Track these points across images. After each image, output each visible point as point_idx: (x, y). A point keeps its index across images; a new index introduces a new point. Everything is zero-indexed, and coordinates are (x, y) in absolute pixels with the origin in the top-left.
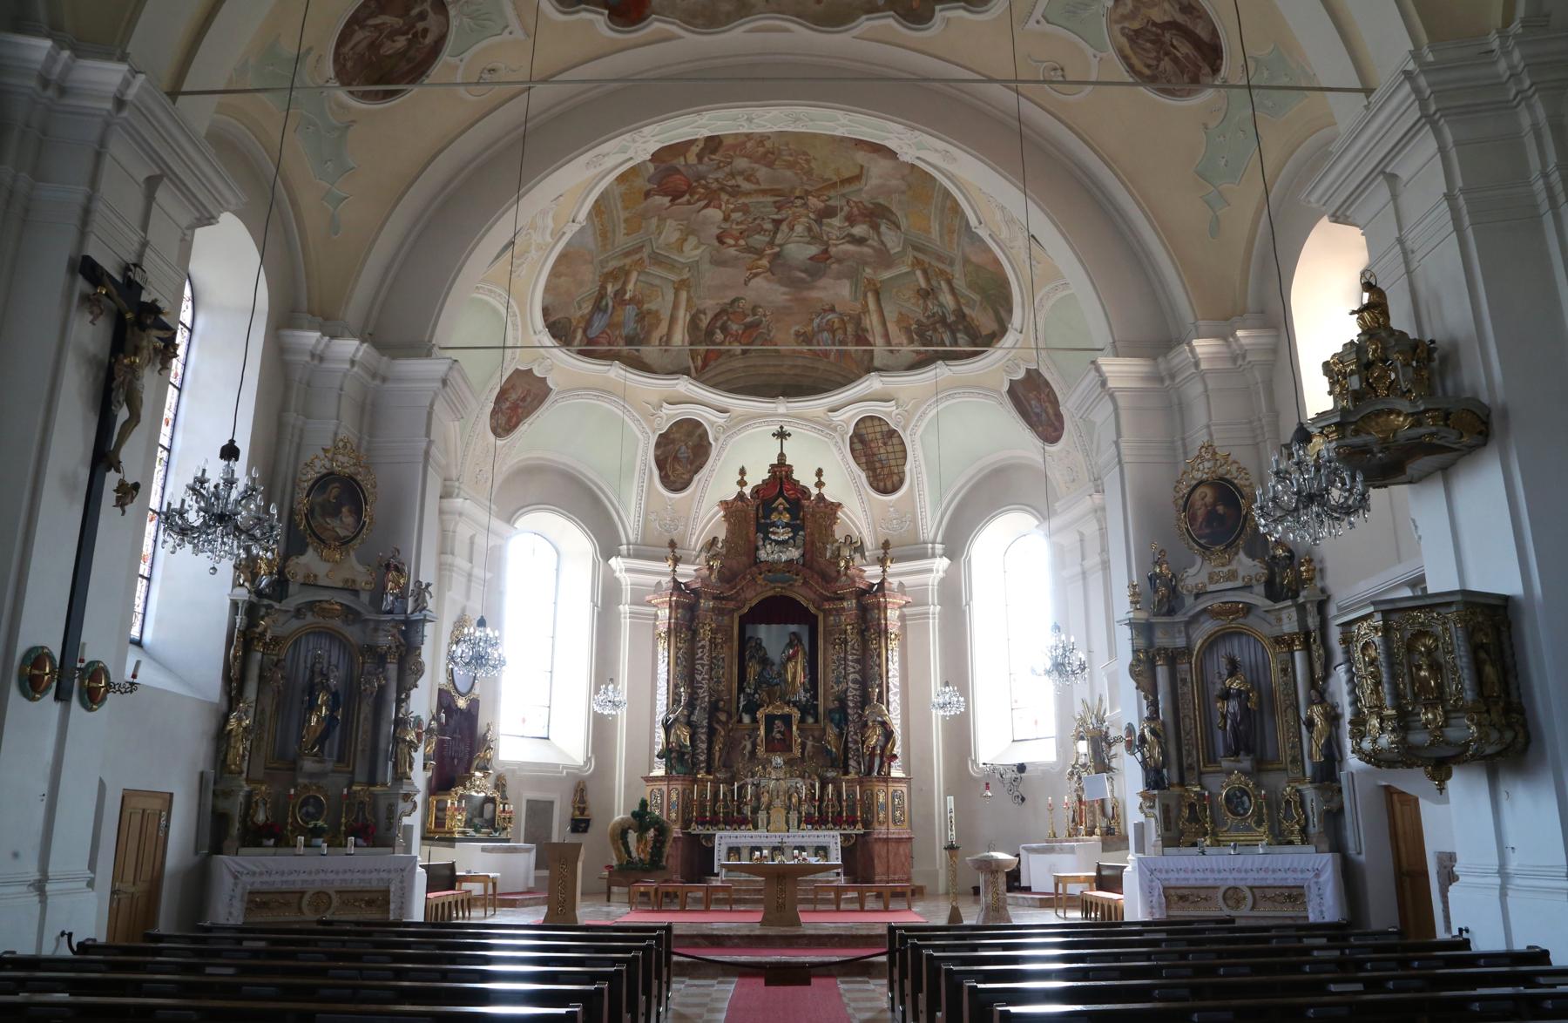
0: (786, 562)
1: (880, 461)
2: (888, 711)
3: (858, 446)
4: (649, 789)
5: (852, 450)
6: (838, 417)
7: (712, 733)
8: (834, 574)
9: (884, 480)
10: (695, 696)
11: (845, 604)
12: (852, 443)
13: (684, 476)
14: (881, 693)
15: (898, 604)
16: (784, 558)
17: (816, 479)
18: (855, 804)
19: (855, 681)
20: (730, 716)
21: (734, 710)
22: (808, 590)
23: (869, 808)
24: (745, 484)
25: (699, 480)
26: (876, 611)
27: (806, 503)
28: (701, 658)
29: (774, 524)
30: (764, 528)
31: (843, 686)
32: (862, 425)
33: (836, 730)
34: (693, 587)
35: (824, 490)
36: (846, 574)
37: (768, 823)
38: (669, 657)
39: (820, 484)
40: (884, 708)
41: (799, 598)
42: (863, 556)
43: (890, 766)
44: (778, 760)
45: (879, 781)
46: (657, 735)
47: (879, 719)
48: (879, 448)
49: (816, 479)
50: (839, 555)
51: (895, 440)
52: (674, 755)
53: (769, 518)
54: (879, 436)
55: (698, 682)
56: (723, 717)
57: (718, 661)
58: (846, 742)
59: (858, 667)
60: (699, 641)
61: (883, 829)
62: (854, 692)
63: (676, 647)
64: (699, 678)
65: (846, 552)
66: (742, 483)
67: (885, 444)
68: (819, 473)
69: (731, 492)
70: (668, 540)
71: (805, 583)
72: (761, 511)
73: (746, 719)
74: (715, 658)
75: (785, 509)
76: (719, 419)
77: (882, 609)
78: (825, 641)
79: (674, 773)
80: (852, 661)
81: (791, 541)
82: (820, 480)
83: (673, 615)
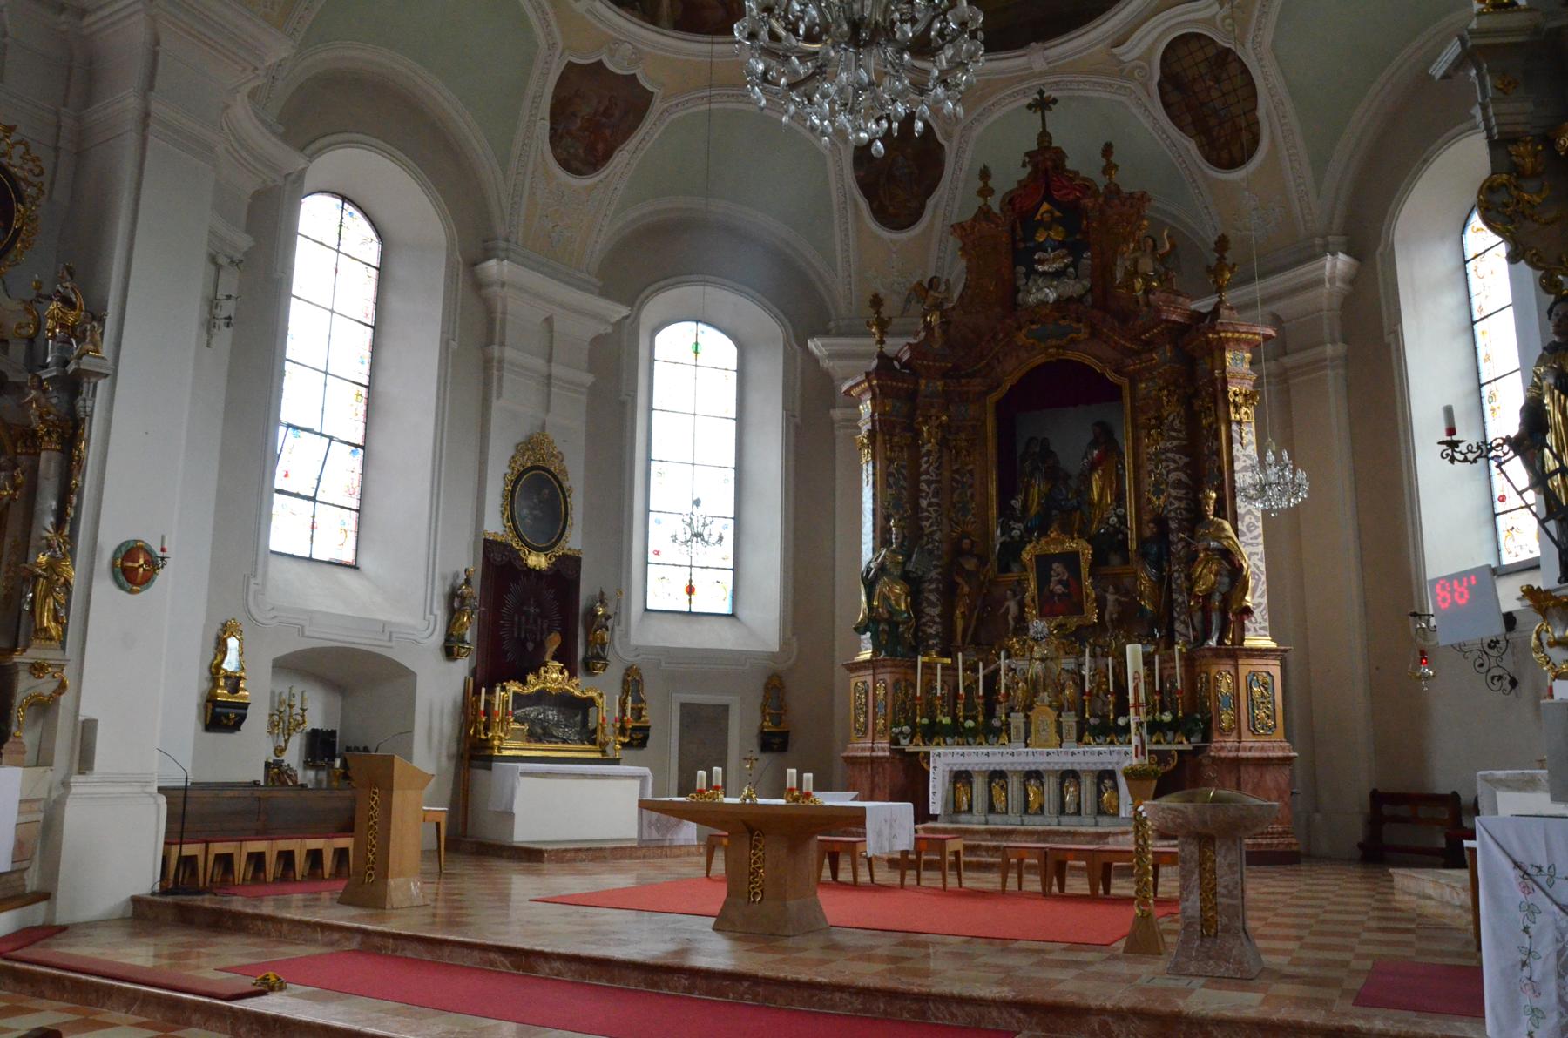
2: (1236, 530)
5: (1167, 106)
6: (1131, 52)
7: (949, 593)
14: (1220, 502)
15: (1248, 342)
17: (1103, 162)
24: (991, 192)
25: (936, 206)
26: (1208, 359)
27: (1088, 202)
28: (927, 472)
29: (1041, 247)
30: (1023, 256)
35: (1117, 177)
36: (1148, 304)
39: (1109, 168)
40: (1227, 525)
41: (1090, 361)
47: (1213, 544)
49: (1103, 162)
52: (882, 626)
54: (1203, 70)
55: (923, 510)
56: (970, 564)
58: (1170, 591)
60: (923, 445)
61: (1230, 742)
63: (887, 459)
64: (924, 503)
66: (986, 192)
67: (1217, 80)
68: (1107, 150)
71: (1094, 334)
74: (957, 471)
81: (1071, 270)
83: (878, 409)
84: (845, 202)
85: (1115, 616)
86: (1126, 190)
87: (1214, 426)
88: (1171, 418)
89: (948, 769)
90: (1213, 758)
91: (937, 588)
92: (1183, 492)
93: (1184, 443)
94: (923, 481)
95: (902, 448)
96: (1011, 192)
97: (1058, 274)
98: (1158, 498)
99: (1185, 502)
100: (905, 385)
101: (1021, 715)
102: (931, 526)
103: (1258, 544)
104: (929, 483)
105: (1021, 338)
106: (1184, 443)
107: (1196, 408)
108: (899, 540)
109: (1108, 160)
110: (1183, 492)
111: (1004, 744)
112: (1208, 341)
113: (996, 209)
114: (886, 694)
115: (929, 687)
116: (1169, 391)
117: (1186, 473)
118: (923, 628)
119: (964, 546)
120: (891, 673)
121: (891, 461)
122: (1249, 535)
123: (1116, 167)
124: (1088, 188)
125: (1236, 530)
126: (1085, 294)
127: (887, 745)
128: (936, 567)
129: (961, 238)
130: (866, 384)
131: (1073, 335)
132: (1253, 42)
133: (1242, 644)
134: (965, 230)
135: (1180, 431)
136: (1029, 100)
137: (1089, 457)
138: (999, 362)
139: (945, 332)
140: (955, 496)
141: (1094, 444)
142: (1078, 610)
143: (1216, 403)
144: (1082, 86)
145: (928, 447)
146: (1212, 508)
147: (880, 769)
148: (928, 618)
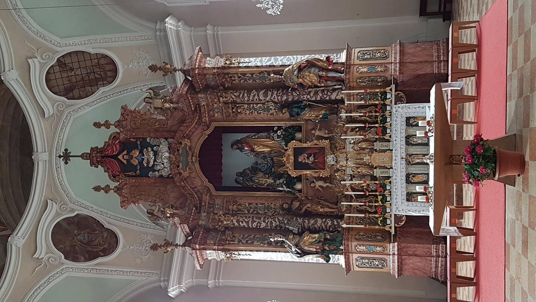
0: (170, 153)
2: (289, 65)
3: (76, 92)
5: (80, 98)
6: (49, 110)
7: (309, 214)
8: (181, 114)
14: (275, 73)
15: (201, 58)
16: (167, 155)
17: (103, 127)
19: (266, 95)
24: (108, 186)
26: (207, 76)
27: (122, 136)
28: (247, 223)
29: (141, 163)
31: (272, 106)
34: (188, 230)
37: (387, 168)
38: (246, 251)
39: (107, 125)
44: (330, 159)
46: (310, 261)
48: (76, 75)
50: (161, 108)
51: (68, 60)
53: (137, 166)
54: (65, 75)
56: (296, 204)
60: (234, 224)
64: (263, 225)
65: (158, 103)
66: (107, 189)
67: (72, 70)
68: (97, 125)
69: (115, 198)
70: (152, 251)
72: (130, 173)
74: (249, 211)
75: (128, 154)
76: (53, 209)
77: (205, 72)
78: (236, 121)
79: (342, 248)
81: (155, 148)
82: (104, 125)
84: (96, 269)
85: (326, 132)
86: (118, 117)
87: (240, 75)
88: (233, 97)
89: (406, 203)
90: (400, 73)
91: (307, 219)
92: (269, 92)
93: (246, 91)
94: (252, 226)
95: (233, 236)
96: (109, 176)
97: (156, 154)
98: (271, 109)
99: (274, 91)
100: (201, 232)
101: (375, 170)
103: (297, 57)
105: (186, 174)
106: (246, 91)
107: (230, 85)
108: (282, 236)
109: (102, 125)
110: (269, 92)
111: (390, 182)
112: (199, 74)
113: (117, 184)
114: (363, 245)
115: (361, 221)
118: (328, 227)
119: (287, 207)
121: (240, 241)
125: (289, 65)
126: (168, 142)
128: (296, 219)
129: (129, 203)
130: (198, 251)
131: (187, 148)
133: (344, 62)
134: (126, 201)
135: (240, 93)
136: (63, 163)
139: (176, 209)
140: (261, 212)
141: (241, 149)
142: (323, 148)
143: (228, 74)
144: (61, 137)
146: (278, 76)
148: (323, 224)
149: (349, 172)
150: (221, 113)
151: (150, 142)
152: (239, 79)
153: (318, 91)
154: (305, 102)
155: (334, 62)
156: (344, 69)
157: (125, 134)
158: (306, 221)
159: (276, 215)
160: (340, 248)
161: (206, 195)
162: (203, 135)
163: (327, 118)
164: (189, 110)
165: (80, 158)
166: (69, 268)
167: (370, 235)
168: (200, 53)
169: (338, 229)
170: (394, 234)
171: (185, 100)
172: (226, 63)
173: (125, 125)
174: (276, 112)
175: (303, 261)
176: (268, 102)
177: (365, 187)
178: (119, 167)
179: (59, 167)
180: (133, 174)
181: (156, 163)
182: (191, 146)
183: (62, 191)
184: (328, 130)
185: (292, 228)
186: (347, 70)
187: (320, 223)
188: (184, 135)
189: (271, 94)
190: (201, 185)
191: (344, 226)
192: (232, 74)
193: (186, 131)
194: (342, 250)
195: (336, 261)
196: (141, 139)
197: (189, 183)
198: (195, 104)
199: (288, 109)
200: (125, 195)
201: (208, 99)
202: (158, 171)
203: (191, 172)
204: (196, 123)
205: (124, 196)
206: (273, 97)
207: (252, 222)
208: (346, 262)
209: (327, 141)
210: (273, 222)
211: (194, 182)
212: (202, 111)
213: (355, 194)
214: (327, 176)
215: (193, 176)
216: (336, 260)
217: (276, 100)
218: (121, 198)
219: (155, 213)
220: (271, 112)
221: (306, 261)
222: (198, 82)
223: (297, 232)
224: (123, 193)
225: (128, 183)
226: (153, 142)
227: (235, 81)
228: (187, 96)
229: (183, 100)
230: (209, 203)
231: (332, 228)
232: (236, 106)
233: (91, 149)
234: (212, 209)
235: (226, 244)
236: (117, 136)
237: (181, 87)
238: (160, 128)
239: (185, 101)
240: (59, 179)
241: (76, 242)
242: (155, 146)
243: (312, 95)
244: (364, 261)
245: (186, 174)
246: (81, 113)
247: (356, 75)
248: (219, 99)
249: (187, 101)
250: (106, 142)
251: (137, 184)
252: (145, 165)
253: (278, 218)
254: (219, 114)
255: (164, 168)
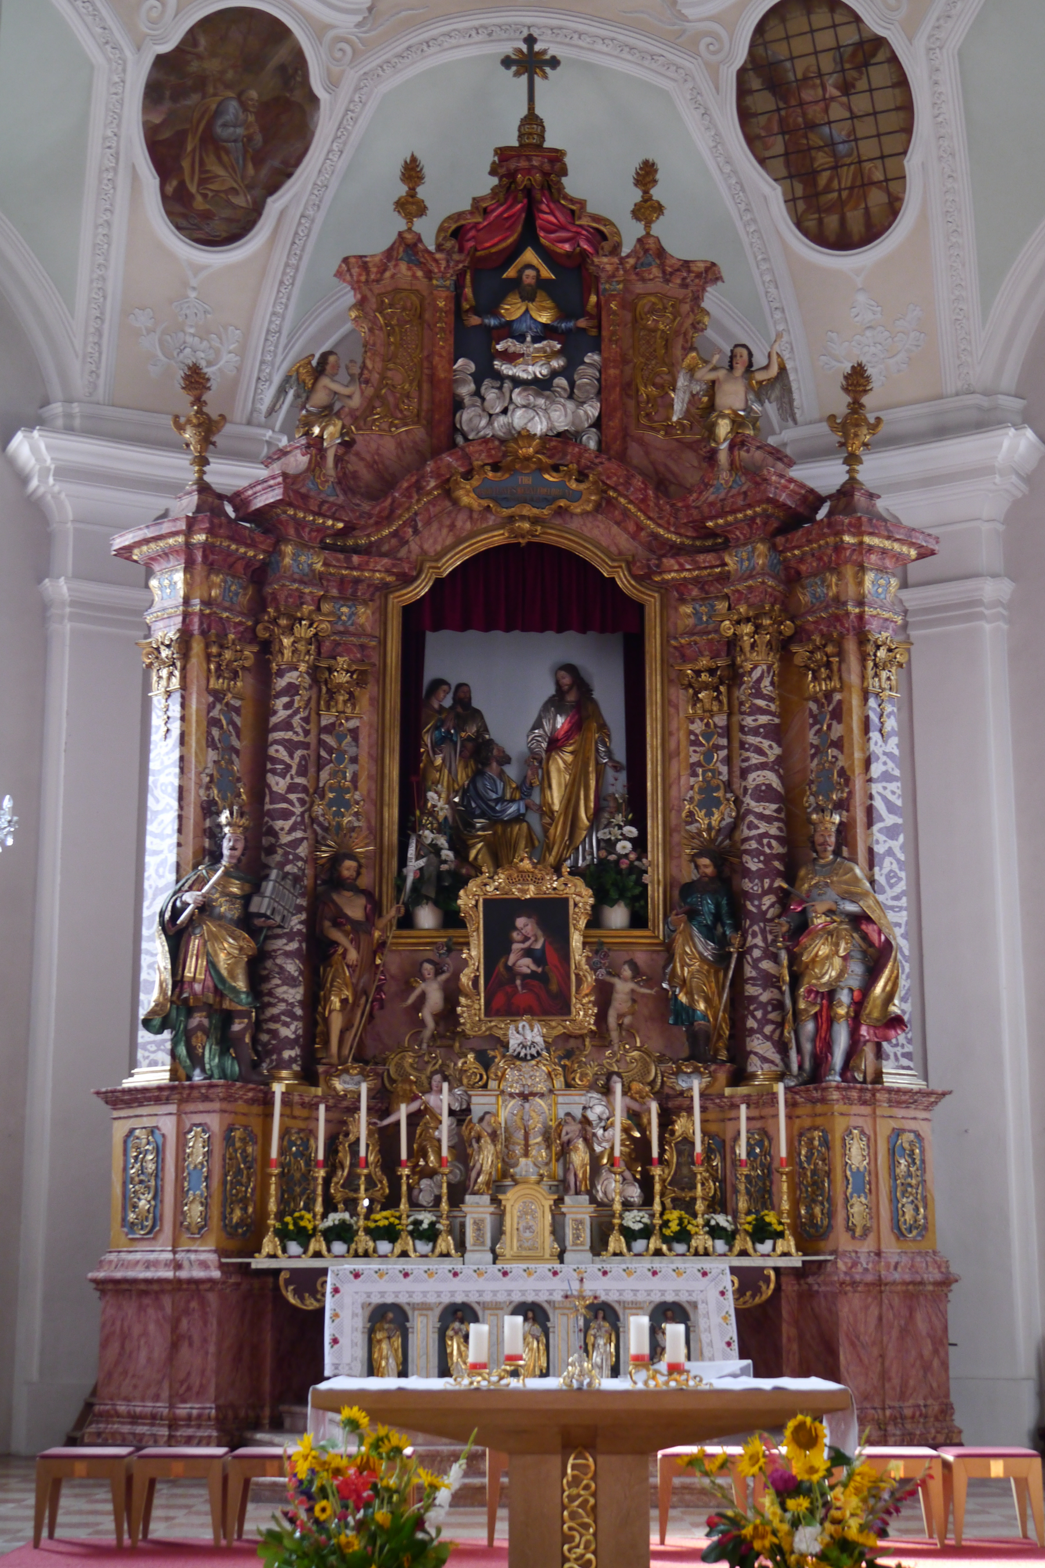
0: (545, 438)
1: (832, 144)
2: (872, 882)
3: (763, 101)
4: (120, 1130)
5: (745, 115)
8: (692, 478)
9: (840, 206)
10: (266, 841)
11: (731, 562)
12: (743, 92)
13: (240, 201)
16: (539, 427)
17: (637, 195)
18: (769, 1172)
20: (375, 908)
21: (388, 891)
22: (615, 529)
23: (817, 1185)
24: (422, 210)
27: (605, 262)
28: (287, 725)
29: (508, 330)
31: (722, 816)
32: (775, 31)
33: (707, 949)
34: (259, 503)
35: (658, 229)
38: (183, 719)
40: (858, 871)
42: (788, 411)
43: (879, 1054)
45: (847, 1100)
46: (145, 960)
48: (827, 101)
49: (637, 195)
50: (711, 407)
51: (879, 75)
53: (496, 314)
54: (827, 63)
56: (355, 909)
57: (340, 739)
58: (739, 980)
59: (774, 751)
60: (280, 674)
62: (763, 827)
64: (278, 784)
67: (846, 88)
71: (605, 506)
72: (468, 291)
73: (427, 917)
74: (329, 729)
75: (542, 284)
78: (667, 681)
80: (755, 732)
81: (561, 382)
82: (647, 198)
83: (197, 592)
84: (115, 170)
85: (627, 1020)
87: (837, 697)
91: (299, 949)
92: (774, 806)
93: (777, 721)
94: (276, 742)
96: (460, 215)
97: (541, 385)
98: (709, 814)
99: (776, 824)
101: (486, 1199)
102: (292, 829)
103: (901, 908)
104: (291, 746)
106: (777, 721)
107: (798, 661)
108: (238, 853)
109: (646, 192)
110: (774, 806)
112: (839, 548)
114: (208, 1154)
116: (758, 628)
117: (776, 772)
118: (273, 1026)
119: (346, 873)
120: (223, 1111)
121: (218, 696)
122: (890, 893)
123: (659, 209)
124: (604, 237)
125: (872, 882)
127: (212, 1257)
128: (299, 909)
129: (356, 286)
130: (181, 539)
132: (930, 37)
133: (882, 1083)
134: (368, 273)
135: (771, 699)
136: (507, 48)
137: (547, 727)
138: (416, 532)
139: (338, 459)
140: (324, 775)
141: (556, 703)
143: (841, 654)
144: (600, 46)
145: (291, 677)
147: (194, 1304)
148: (282, 1006)
149: (480, 1103)
150: (695, 626)
151: (584, 363)
152: (820, 695)
153: (780, 988)
154: (737, 941)
155: (885, 1044)
156: (855, 1081)
157: (614, 276)
158: (294, 946)
159: (315, 832)
160: (197, 1072)
161: (388, 571)
162: (613, 560)
163: (676, 1023)
164: (706, 510)
165: (524, 112)
166: (124, 71)
167: (244, 1180)
168: (913, 553)
169: (264, 1065)
170: (253, 1266)
171: (745, 493)
172: (878, 647)
173: (646, 275)
174: (699, 834)
175: (145, 932)
176: (738, 802)
177: (422, 1163)
178: (493, 250)
179: (490, 35)
180: (466, 300)
181: (507, 385)
182: (572, 515)
183: (406, 45)
184: (631, 1026)
185: (268, 893)
186: (854, 1094)
187: (285, 996)
188: (615, 489)
189: (767, 812)
190: (424, 552)
191: (278, 1089)
192: (839, 670)
193: (626, 497)
194: (189, 1078)
195: (147, 1054)
196: (593, 332)
197: (434, 506)
198: (729, 532)
199: (712, 879)
200: (388, 274)
201: (746, 580)
202: (477, 393)
203: (475, 516)
204: (655, 536)
205: (385, 270)
206: (756, 822)
207: (289, 741)
208: (145, 1090)
209: (590, 1023)
210: (290, 822)
211: (435, 526)
212: (701, 558)
213: (397, 1124)
214: (460, 1024)
215: (459, 524)
216: (152, 1056)
217: (747, 833)
218: (377, 259)
219: (325, 381)
220: (700, 815)
221: (145, 945)
222: (809, 542)
223: (253, 908)
224: (396, 265)
225: (435, 282)
226: (586, 377)
227: (815, 678)
228: (759, 503)
229: (744, 488)
230: (357, 581)
231: (268, 1043)
232: (722, 683)
233: (556, 151)
234: (334, 592)
235: (207, 646)
236: (606, 246)
237: (791, 480)
238: (638, 403)
239: (739, 494)
240: (448, 35)
241: (215, 95)
242: (572, 384)
243: (766, 965)
244: (150, 1157)
245: (467, 497)
246: (690, 118)
247: (840, 1125)
248: (748, 620)
249: (740, 502)
250: (582, 204)
251: (427, 316)
252: (498, 347)
253: (302, 839)
254: (691, 621)
255: (490, 415)
